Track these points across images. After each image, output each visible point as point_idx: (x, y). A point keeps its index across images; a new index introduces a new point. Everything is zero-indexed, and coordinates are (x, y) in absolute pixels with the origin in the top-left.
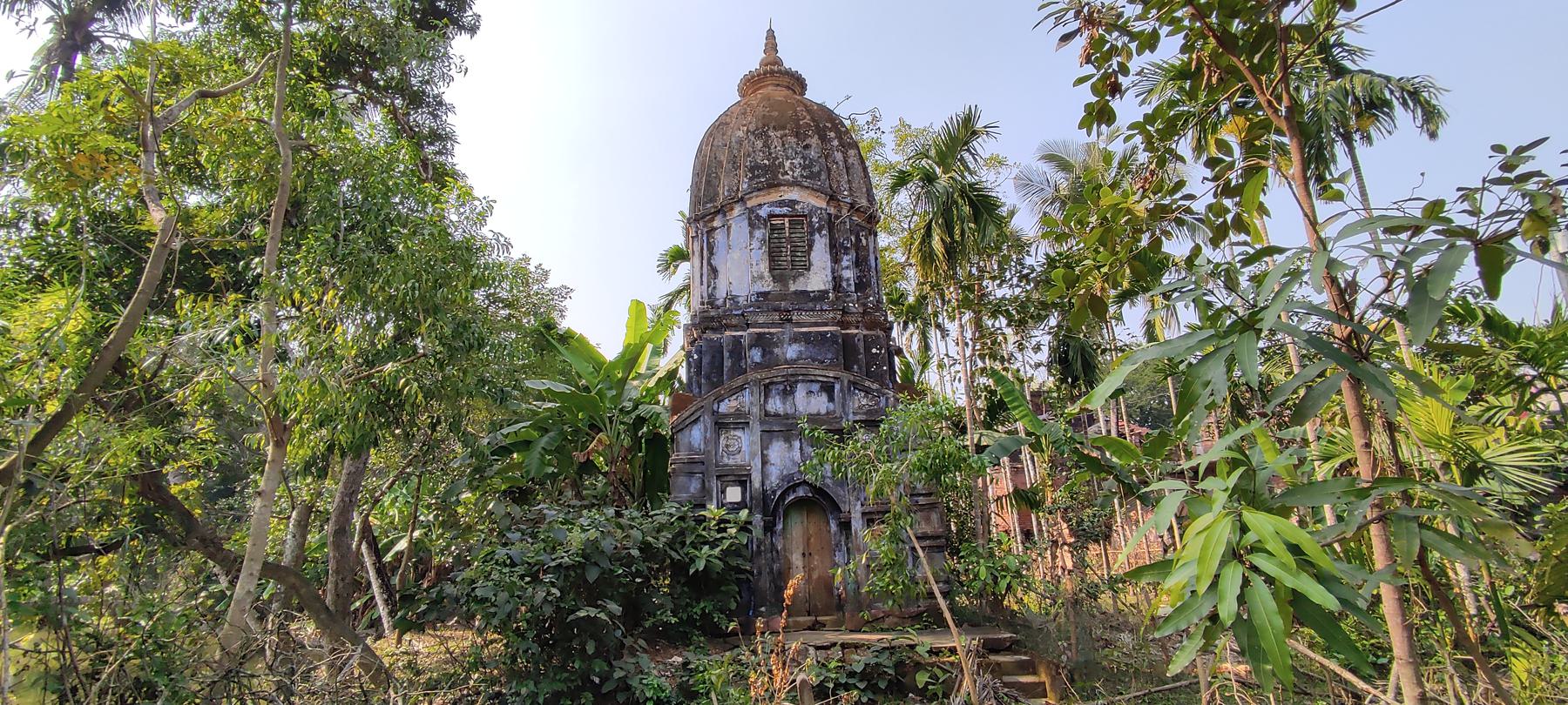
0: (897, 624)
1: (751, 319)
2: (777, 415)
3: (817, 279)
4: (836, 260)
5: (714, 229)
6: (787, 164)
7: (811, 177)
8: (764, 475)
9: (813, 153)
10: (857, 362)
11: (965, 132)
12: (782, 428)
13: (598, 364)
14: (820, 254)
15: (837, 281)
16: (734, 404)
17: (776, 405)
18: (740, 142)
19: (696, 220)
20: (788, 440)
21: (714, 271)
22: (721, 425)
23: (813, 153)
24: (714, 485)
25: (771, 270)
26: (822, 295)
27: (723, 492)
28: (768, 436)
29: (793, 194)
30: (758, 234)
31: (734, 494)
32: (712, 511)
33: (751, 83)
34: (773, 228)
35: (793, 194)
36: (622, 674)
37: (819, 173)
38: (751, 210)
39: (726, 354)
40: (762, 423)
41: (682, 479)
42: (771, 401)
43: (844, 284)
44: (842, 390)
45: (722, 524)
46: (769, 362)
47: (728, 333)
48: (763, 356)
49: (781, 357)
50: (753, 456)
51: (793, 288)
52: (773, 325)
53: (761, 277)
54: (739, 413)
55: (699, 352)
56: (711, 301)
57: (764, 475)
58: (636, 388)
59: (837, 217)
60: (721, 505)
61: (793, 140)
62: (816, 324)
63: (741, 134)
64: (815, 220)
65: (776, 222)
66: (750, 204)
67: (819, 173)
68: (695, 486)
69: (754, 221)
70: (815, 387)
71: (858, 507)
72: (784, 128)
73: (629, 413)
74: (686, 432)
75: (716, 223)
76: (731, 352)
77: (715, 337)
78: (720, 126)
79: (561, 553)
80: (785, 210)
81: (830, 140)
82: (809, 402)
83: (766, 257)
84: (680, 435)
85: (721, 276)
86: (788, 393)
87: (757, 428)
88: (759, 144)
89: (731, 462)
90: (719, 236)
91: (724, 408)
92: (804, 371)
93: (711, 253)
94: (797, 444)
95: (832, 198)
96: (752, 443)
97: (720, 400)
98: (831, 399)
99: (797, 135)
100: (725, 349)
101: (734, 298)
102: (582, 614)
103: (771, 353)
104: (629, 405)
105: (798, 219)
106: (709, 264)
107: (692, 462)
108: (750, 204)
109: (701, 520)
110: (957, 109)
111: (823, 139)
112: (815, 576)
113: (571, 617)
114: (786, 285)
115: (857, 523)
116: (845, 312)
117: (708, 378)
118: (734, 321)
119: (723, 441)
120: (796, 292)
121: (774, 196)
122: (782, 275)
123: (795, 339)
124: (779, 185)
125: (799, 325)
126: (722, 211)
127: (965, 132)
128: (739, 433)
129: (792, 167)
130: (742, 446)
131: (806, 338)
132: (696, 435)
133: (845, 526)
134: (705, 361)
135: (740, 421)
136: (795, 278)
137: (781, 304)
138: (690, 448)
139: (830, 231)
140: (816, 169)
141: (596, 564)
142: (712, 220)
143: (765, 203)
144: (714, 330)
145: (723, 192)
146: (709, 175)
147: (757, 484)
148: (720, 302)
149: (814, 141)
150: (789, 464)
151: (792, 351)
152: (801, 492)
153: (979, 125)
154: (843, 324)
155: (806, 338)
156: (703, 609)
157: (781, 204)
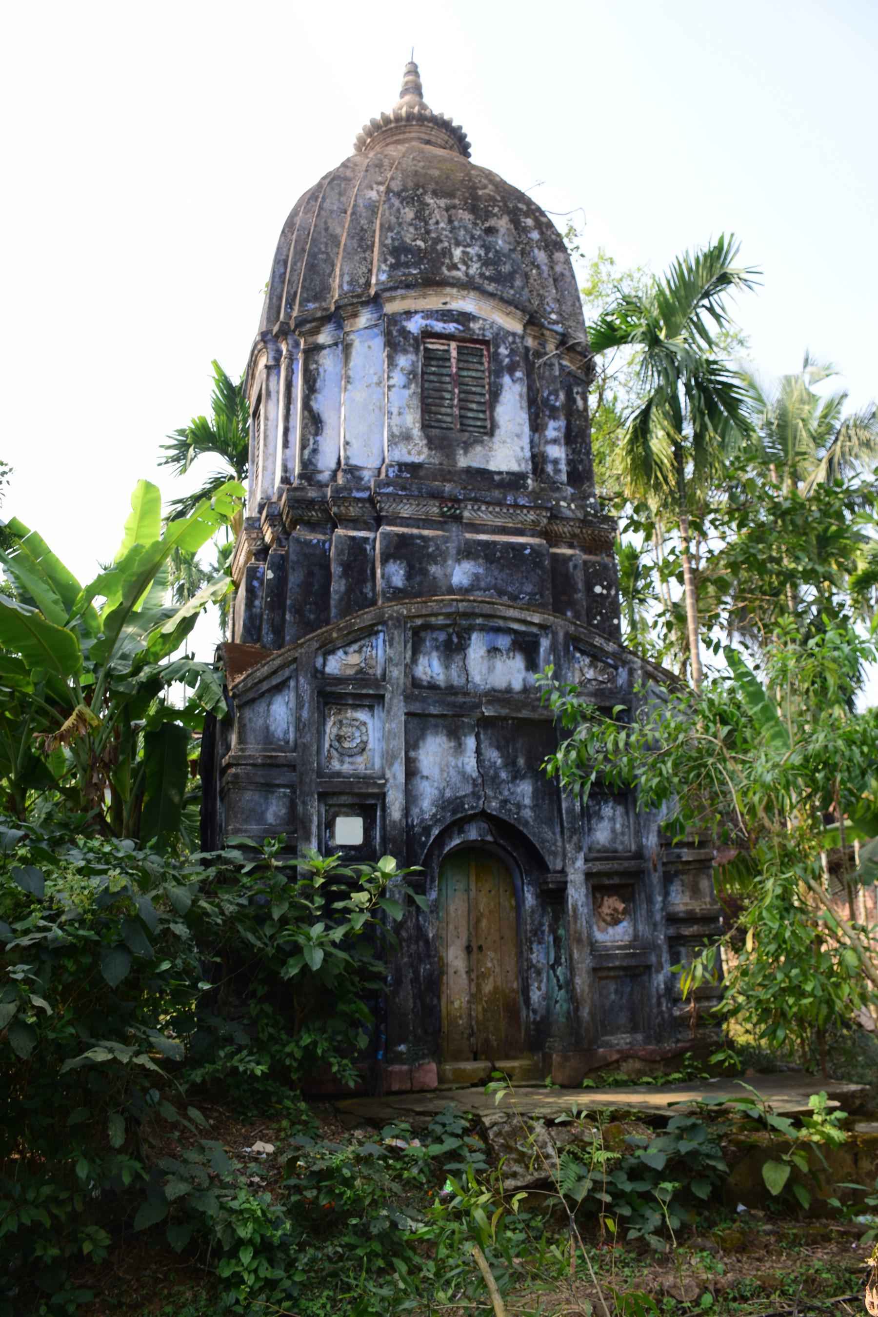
0: (641, 1073)
1: (387, 508)
2: (433, 687)
3: (506, 451)
4: (536, 427)
5: (319, 348)
6: (457, 252)
7: (499, 279)
8: (410, 798)
9: (500, 243)
10: (571, 604)
11: (711, 273)
12: (443, 711)
13: (66, 591)
14: (511, 409)
15: (538, 460)
16: (354, 659)
17: (431, 668)
18: (373, 208)
19: (284, 333)
20: (455, 734)
21: (314, 422)
22: (331, 696)
23: (500, 243)
24: (315, 810)
25: (425, 427)
26: (514, 481)
27: (330, 825)
28: (418, 725)
29: (467, 304)
30: (404, 361)
31: (349, 831)
32: (312, 859)
33: (384, 131)
34: (430, 357)
35: (467, 304)
36: (183, 1188)
37: (511, 276)
38: (393, 319)
39: (336, 569)
40: (408, 698)
41: (249, 797)
42: (423, 661)
43: (550, 468)
44: (553, 648)
45: (337, 887)
46: (420, 584)
47: (340, 531)
48: (409, 576)
49: (442, 583)
50: (389, 758)
51: (463, 462)
52: (427, 523)
53: (407, 437)
54: (362, 677)
55: (281, 566)
56: (309, 470)
57: (410, 798)
58: (132, 637)
59: (538, 355)
60: (327, 851)
61: (466, 216)
62: (503, 531)
63: (373, 195)
64: (503, 351)
65: (435, 345)
66: (390, 308)
67: (511, 276)
68: (274, 811)
69: (395, 339)
70: (504, 641)
71: (580, 863)
72: (451, 195)
73: (122, 678)
74: (261, 707)
75: (323, 338)
76: (347, 568)
77: (315, 537)
78: (336, 181)
79: (36, 918)
80: (451, 327)
81: (526, 230)
82: (492, 669)
83: (416, 402)
84: (248, 713)
85: (328, 432)
86: (454, 649)
87: (399, 708)
88: (409, 214)
89: (346, 768)
90: (328, 362)
91: (336, 664)
92: (487, 609)
93: (311, 387)
94: (471, 742)
95: (533, 321)
96: (387, 736)
97: (328, 649)
98: (532, 665)
99: (474, 210)
100: (315, 568)
101: (353, 471)
102: (100, 1055)
103: (424, 572)
104: (125, 669)
105: (475, 344)
106: (307, 405)
107: (271, 764)
108: (390, 308)
109: (292, 873)
110: (701, 244)
111: (516, 222)
112: (488, 987)
113: (75, 1062)
114: (451, 456)
115: (577, 894)
116: (555, 516)
117: (298, 611)
118: (354, 511)
119: (331, 730)
120: (469, 471)
121: (433, 302)
122: (443, 438)
123: (468, 552)
124: (444, 283)
125: (474, 527)
126: (337, 317)
127: (711, 273)
128: (362, 715)
129: (464, 259)
130: (370, 739)
131: (486, 553)
132: (280, 714)
133: (554, 897)
134: (295, 579)
135: (366, 692)
136: (467, 447)
137: (441, 485)
138: (268, 737)
139: (529, 374)
140: (506, 268)
141: (122, 946)
142: (316, 331)
143: (418, 310)
144: (312, 526)
145: (338, 285)
146: (313, 256)
147: (396, 813)
148: (325, 476)
149: (503, 223)
150: (455, 779)
151: (461, 573)
152: (473, 834)
153: (734, 265)
154: (552, 538)
155: (486, 553)
156: (309, 1051)
157: (446, 316)
